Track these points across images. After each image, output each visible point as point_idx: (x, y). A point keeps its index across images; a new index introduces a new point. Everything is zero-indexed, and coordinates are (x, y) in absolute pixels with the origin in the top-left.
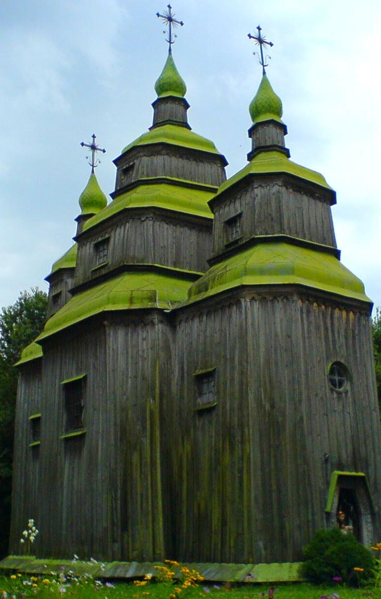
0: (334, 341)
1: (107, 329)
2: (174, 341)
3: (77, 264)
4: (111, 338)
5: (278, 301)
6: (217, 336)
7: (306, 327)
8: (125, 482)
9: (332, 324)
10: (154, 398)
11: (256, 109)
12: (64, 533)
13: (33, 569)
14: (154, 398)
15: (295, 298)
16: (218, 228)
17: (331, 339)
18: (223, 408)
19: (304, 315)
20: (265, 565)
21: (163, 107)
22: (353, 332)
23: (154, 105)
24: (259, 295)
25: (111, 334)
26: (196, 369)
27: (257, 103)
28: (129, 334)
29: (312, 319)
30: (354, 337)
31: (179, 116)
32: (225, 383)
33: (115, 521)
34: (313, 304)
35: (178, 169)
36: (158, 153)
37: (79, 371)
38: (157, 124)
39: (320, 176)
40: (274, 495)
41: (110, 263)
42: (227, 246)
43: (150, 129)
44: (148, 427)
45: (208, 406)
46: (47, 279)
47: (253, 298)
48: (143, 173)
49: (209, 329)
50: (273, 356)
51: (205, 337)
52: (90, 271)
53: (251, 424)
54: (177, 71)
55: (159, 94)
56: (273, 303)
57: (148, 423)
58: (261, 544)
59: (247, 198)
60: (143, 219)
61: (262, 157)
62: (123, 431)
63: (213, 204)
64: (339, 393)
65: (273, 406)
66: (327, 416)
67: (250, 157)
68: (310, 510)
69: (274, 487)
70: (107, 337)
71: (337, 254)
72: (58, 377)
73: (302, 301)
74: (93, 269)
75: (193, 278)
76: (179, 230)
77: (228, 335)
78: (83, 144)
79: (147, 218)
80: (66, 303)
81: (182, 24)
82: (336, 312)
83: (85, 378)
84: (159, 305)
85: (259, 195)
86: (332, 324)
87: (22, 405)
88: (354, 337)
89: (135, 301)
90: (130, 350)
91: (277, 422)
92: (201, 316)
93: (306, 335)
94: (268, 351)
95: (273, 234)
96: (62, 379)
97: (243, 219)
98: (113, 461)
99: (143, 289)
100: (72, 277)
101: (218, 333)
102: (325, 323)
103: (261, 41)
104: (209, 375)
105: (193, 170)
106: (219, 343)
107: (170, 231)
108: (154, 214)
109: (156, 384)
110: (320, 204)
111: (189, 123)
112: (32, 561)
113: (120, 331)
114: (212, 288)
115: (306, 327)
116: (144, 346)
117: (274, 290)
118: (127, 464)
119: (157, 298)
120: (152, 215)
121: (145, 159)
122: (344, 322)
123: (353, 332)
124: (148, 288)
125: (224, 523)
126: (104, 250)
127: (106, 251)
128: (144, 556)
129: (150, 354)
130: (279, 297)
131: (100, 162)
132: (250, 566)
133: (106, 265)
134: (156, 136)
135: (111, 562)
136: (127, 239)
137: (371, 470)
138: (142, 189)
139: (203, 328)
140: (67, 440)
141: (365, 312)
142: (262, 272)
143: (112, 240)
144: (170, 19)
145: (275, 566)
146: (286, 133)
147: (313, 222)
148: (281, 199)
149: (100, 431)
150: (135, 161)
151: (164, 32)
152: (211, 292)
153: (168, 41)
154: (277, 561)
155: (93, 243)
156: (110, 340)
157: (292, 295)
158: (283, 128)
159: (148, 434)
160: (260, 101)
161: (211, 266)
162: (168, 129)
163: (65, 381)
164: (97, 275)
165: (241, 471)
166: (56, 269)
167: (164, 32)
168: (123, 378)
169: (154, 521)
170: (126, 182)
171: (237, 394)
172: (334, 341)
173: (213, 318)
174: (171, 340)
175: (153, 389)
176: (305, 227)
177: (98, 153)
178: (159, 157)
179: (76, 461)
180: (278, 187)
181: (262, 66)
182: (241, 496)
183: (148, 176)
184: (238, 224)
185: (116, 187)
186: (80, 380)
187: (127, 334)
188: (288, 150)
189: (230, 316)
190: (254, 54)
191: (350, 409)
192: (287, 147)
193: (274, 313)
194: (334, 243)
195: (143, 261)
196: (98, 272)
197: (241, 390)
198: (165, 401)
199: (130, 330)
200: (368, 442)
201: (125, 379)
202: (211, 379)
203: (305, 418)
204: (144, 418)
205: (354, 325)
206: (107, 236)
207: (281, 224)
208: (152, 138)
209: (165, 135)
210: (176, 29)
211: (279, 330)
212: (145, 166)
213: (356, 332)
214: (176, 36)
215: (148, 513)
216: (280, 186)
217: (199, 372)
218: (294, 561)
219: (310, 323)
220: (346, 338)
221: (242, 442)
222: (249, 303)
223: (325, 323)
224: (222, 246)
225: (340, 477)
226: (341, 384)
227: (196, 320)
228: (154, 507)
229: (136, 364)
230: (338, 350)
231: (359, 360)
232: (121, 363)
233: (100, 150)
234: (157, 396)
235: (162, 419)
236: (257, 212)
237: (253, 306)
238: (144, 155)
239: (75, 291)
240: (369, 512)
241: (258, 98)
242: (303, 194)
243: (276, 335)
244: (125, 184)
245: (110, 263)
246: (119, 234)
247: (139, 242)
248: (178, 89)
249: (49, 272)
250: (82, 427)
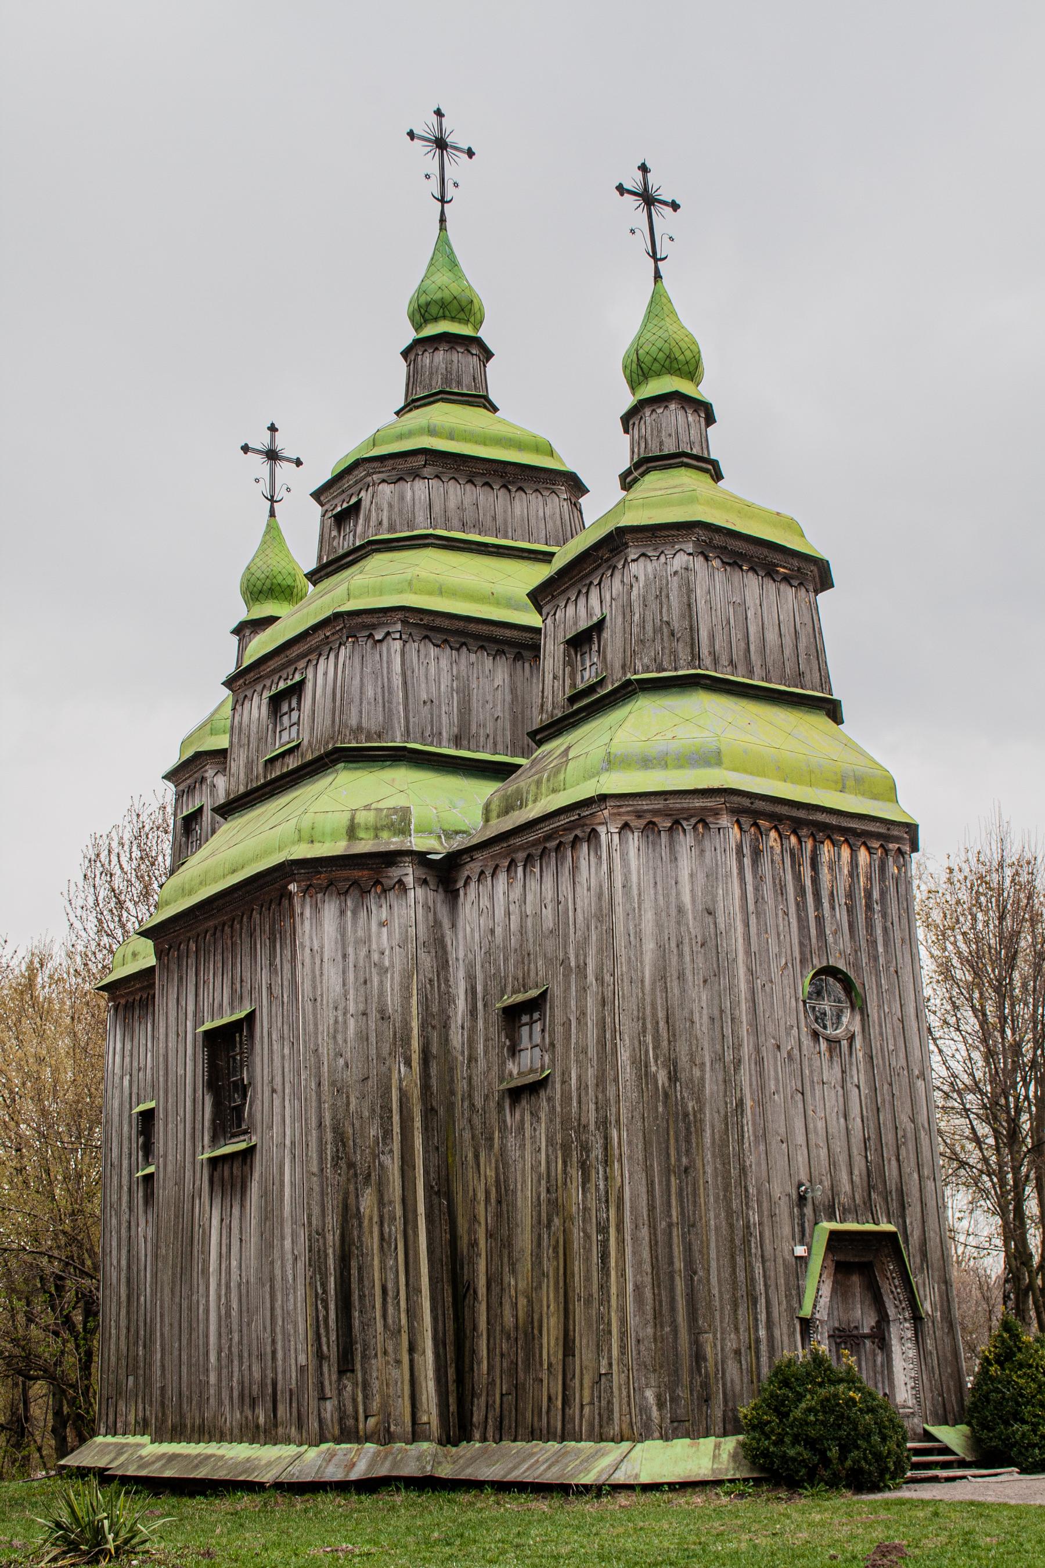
0: (820, 920)
1: (296, 901)
2: (454, 926)
3: (231, 742)
4: (307, 923)
5: (684, 830)
6: (548, 913)
7: (750, 888)
8: (344, 1259)
9: (815, 881)
10: (408, 1063)
11: (639, 365)
12: (213, 1379)
13: (141, 1467)
14: (408, 1063)
15: (725, 821)
16: (552, 651)
17: (812, 914)
18: (563, 1082)
19: (747, 861)
20: (659, 1443)
21: (426, 359)
22: (869, 895)
23: (405, 354)
24: (639, 817)
25: (307, 913)
26: (503, 994)
27: (641, 352)
28: (349, 913)
29: (766, 868)
30: (869, 907)
31: (466, 380)
32: (567, 1024)
33: (325, 1348)
34: (767, 835)
35: (464, 510)
36: (416, 475)
37: (236, 998)
38: (414, 401)
39: (792, 526)
40: (680, 1285)
41: (305, 742)
42: (572, 699)
43: (397, 413)
44: (396, 1129)
45: (532, 1078)
46: (169, 776)
47: (626, 826)
48: (380, 523)
49: (530, 898)
50: (674, 959)
51: (523, 917)
52: (262, 761)
53: (624, 1120)
54: (461, 271)
55: (418, 328)
56: (671, 837)
57: (396, 1118)
58: (650, 1394)
59: (615, 585)
60: (378, 637)
61: (654, 482)
62: (340, 1137)
63: (540, 596)
64: (833, 1043)
65: (673, 1077)
66: (803, 1094)
67: (628, 481)
68: (763, 1317)
69: (679, 1264)
70: (298, 919)
71: (833, 710)
72: (190, 1016)
73: (741, 829)
74: (268, 757)
75: (501, 771)
76: (466, 658)
77: (571, 914)
78: (246, 449)
79: (388, 634)
80: (213, 832)
81: (470, 153)
82: (826, 849)
83: (251, 1017)
84: (418, 843)
85: (642, 578)
86: (815, 881)
87: (117, 1079)
88: (869, 907)
89: (362, 834)
90: (350, 950)
91: (686, 1115)
92: (512, 864)
93: (751, 907)
94: (661, 949)
95: (676, 669)
96: (198, 1022)
97: (606, 634)
98: (316, 1210)
99: (381, 805)
100: (223, 770)
101: (549, 907)
103: (648, 199)
104: (536, 1005)
105: (499, 511)
106: (551, 932)
107: (444, 663)
108: (405, 622)
109: (411, 1029)
110: (789, 592)
111: (491, 397)
112: (142, 1446)
113: (326, 905)
114: (535, 801)
115: (750, 888)
116: (383, 939)
117: (674, 803)
118: (348, 1214)
119: (412, 827)
120: (399, 627)
121: (386, 489)
122: (846, 872)
123: (869, 895)
124: (390, 803)
125: (568, 1348)
126: (291, 710)
127: (295, 715)
128: (392, 1428)
129: (397, 961)
130: (687, 819)
131: (288, 490)
132: (626, 1445)
133: (298, 746)
134: (410, 434)
135: (317, 1446)
136: (343, 686)
138: (378, 563)
139: (516, 893)
140: (214, 1162)
141: (897, 846)
142: (646, 762)
143: (309, 685)
144: (441, 144)
145: (681, 1445)
146: (710, 420)
147: (771, 636)
148: (692, 586)
149: (288, 1142)
150: (363, 494)
151: (427, 177)
152: (533, 811)
153: (438, 199)
154: (687, 1435)
155: (266, 694)
156: (305, 929)
157: (716, 813)
158: (706, 412)
159: (396, 1146)
160: (646, 348)
161: (540, 743)
162: (442, 414)
163: (208, 1026)
164: (277, 773)
165: (603, 1229)
166: (189, 753)
167: (427, 177)
168: (336, 1017)
169: (412, 1350)
170: (345, 544)
171: (592, 1052)
172: (820, 920)
173: (537, 870)
174: (446, 924)
175: (406, 1041)
176: (752, 648)
177: (284, 470)
178: (420, 485)
179: (236, 1211)
180: (686, 557)
181: (652, 261)
182: (604, 1287)
183: (392, 529)
184: (595, 647)
185: (320, 558)
186: (237, 1025)
187: (342, 912)
188: (715, 464)
189: (575, 869)
190: (633, 231)
191: (859, 1075)
192: (713, 456)
193: (676, 859)
194: (825, 682)
195: (379, 736)
196: (278, 764)
197: (602, 1042)
198: (434, 1071)
199: (349, 903)
200: (903, 1152)
201: (340, 1019)
202: (536, 1016)
203: (748, 1103)
204: (387, 1108)
205: (869, 879)
206: (298, 678)
207: (693, 644)
208: (401, 437)
209: (432, 432)
210: (457, 167)
211: (687, 899)
212: (385, 507)
213: (876, 895)
214: (456, 185)
215: (399, 1331)
216: (690, 554)
217: (509, 1000)
218: (725, 1434)
219: (759, 879)
220: (850, 910)
221: (607, 1162)
222: (616, 837)
223: (798, 877)
224: (561, 698)
225: (835, 1236)
227: (502, 877)
228: (413, 1313)
229: (365, 982)
230: (830, 939)
231: (882, 960)
232: (332, 977)
233: (288, 460)
234: (415, 1058)
235: (429, 1112)
236: (636, 617)
237: (627, 842)
238: (384, 481)
239: (229, 809)
240: (907, 1315)
241: (642, 340)
242: (748, 571)
243: (680, 910)
244: (341, 552)
245: (305, 742)
246: (325, 674)
247: (370, 693)
248: (462, 315)
249: (172, 760)
250: (245, 1132)
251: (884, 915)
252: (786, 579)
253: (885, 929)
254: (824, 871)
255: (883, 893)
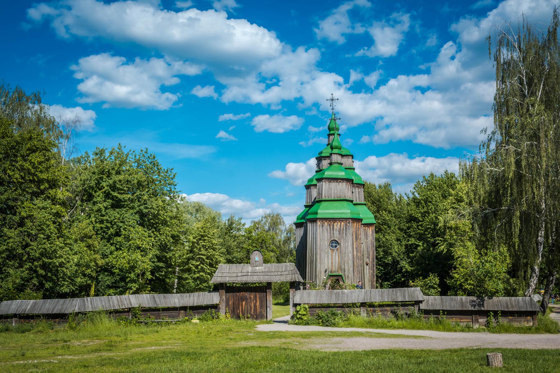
9: (333, 228)
17: (332, 233)
19: (321, 227)
22: (343, 229)
29: (324, 227)
30: (343, 230)
88: (343, 230)
102: (330, 228)
123: (343, 229)
137: (346, 273)
144: (332, 100)
172: (333, 233)
205: (343, 226)
223: (330, 228)
226: (336, 246)
251: (346, 231)
252: (340, 182)
253: (346, 233)
254: (335, 226)
255: (346, 228)
